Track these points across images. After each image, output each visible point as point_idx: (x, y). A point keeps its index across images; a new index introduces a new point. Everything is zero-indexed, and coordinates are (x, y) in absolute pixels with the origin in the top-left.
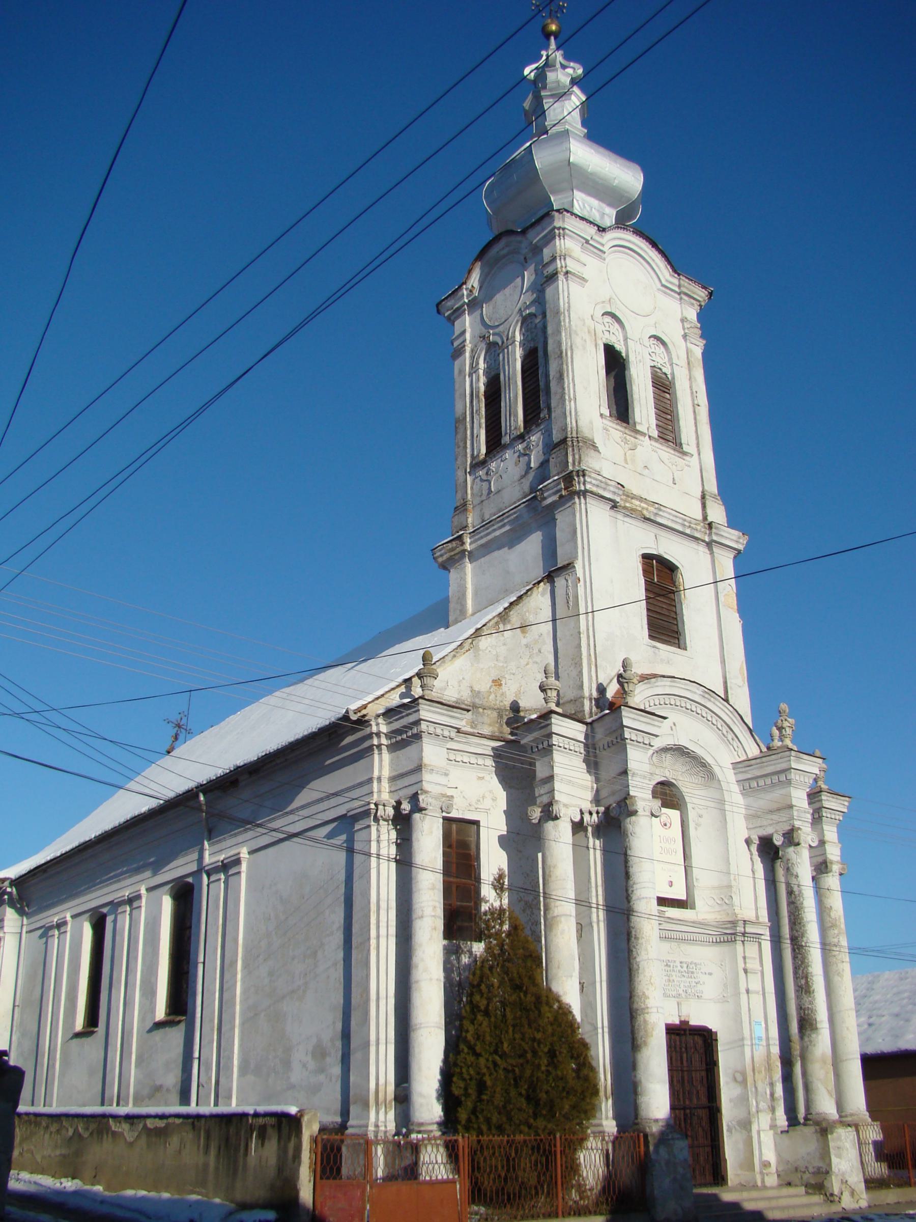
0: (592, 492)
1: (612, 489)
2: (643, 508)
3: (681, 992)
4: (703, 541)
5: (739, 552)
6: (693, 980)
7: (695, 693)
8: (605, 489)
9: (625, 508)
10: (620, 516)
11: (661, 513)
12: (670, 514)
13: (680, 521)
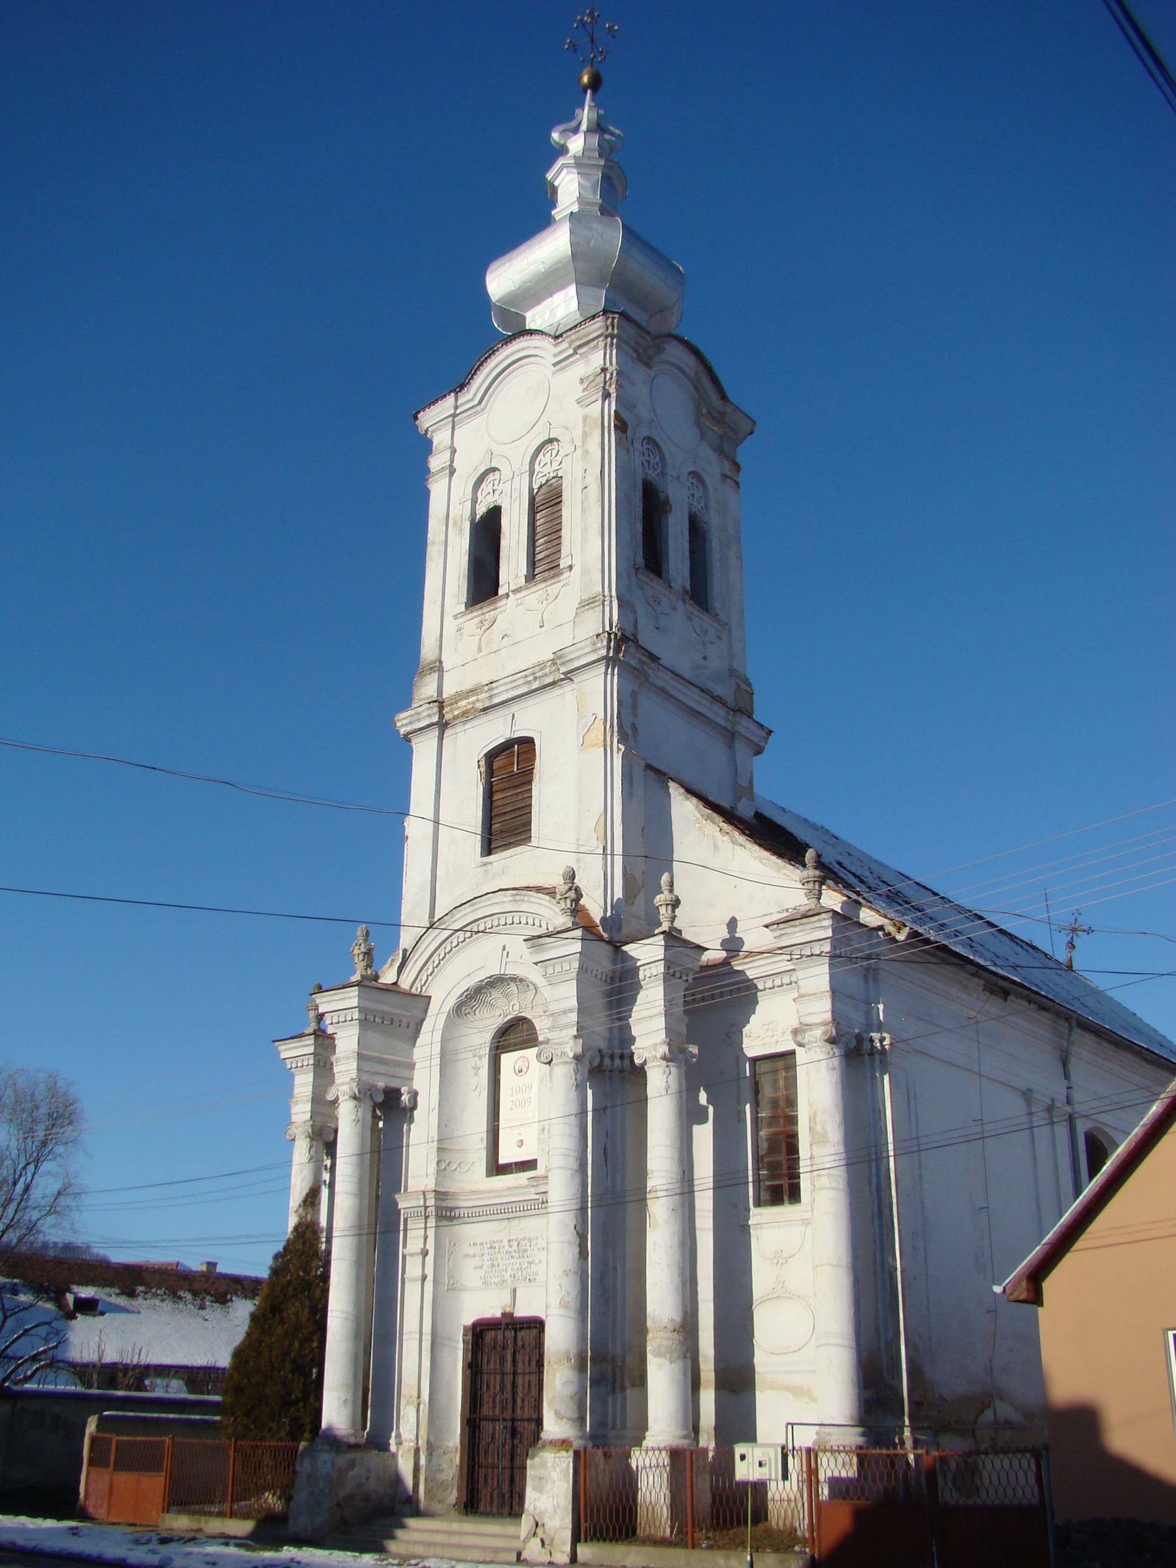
0: (409, 733)
1: (425, 714)
2: (473, 703)
3: (507, 1277)
4: (562, 680)
5: (606, 658)
6: (526, 1260)
7: (503, 902)
8: (419, 720)
9: (455, 718)
10: (459, 728)
11: (495, 692)
12: (505, 684)
13: (522, 681)
